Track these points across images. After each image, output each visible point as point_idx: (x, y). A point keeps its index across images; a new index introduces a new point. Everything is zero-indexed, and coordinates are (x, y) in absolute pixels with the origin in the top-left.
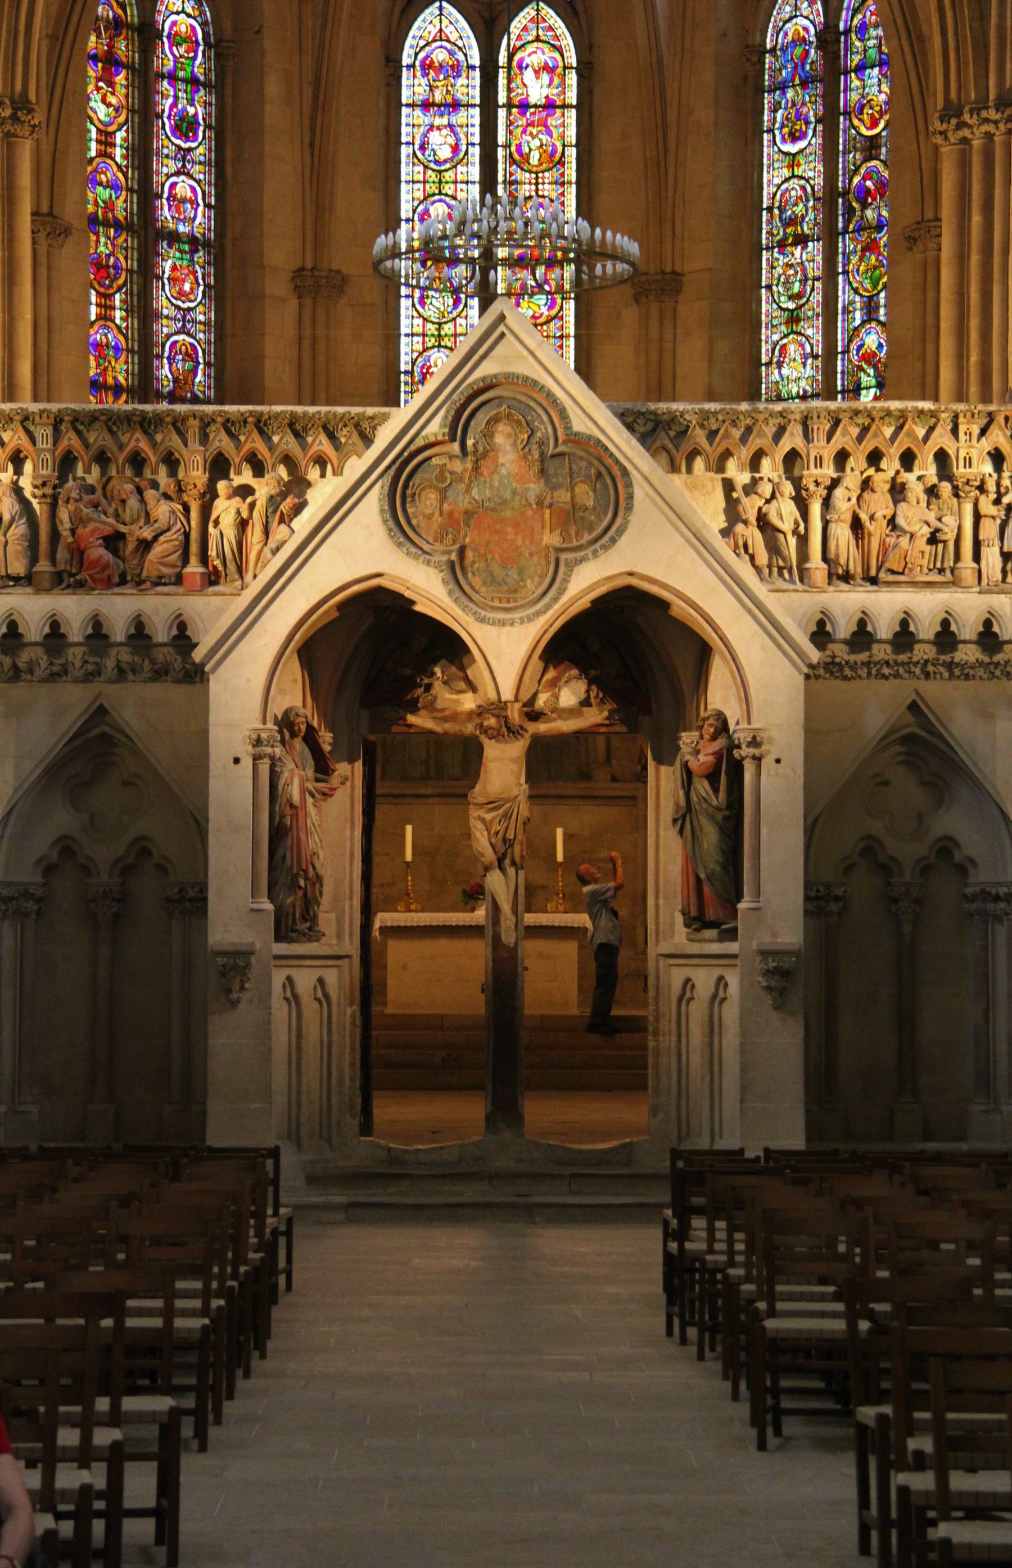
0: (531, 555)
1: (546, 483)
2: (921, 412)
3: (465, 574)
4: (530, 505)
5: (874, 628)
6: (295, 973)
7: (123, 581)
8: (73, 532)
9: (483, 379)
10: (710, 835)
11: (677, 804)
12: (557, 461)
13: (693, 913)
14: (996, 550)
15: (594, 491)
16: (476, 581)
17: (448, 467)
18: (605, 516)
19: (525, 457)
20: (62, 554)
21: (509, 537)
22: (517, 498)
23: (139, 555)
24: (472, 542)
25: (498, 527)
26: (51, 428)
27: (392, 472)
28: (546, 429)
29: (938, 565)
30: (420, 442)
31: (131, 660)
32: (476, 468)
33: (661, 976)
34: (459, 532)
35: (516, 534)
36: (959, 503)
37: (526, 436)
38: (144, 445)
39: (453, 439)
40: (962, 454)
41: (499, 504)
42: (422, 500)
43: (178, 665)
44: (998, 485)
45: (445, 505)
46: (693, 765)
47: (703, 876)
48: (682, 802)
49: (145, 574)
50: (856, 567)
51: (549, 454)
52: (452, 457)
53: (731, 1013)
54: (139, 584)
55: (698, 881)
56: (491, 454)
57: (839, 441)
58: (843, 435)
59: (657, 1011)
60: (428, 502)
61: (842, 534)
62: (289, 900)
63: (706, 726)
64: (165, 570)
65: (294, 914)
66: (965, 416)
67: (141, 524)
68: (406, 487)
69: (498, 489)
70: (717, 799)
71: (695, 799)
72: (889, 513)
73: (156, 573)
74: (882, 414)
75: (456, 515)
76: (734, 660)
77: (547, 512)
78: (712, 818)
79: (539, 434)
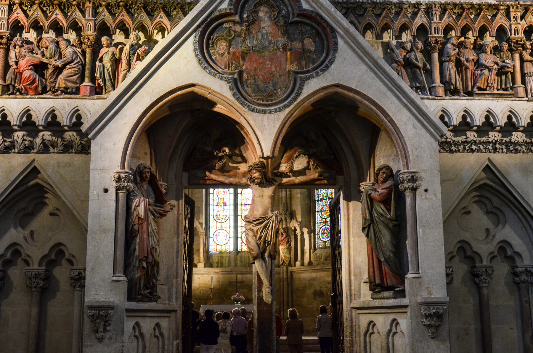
1: (288, 37)
3: (243, 86)
4: (279, 49)
6: (141, 321)
7: (44, 91)
8: (17, 63)
10: (386, 237)
11: (365, 219)
13: (378, 281)
15: (315, 42)
16: (249, 90)
17: (233, 28)
19: (276, 24)
22: (272, 45)
23: (55, 76)
24: (246, 69)
25: (261, 61)
26: (7, 7)
27: (200, 29)
28: (287, 9)
29: (503, 86)
30: (217, 13)
31: (51, 139)
32: (248, 30)
33: (354, 320)
35: (271, 65)
37: (276, 13)
38: (60, 17)
39: (236, 14)
40: (513, 27)
41: (262, 49)
42: (218, 46)
45: (231, 49)
46: (375, 195)
47: (382, 260)
48: (368, 217)
49: (57, 86)
50: (459, 85)
52: (235, 23)
54: (54, 92)
55: (379, 261)
56: (257, 22)
58: (449, 18)
60: (221, 47)
61: (451, 67)
62: (137, 276)
63: (381, 173)
64: (70, 85)
65: (140, 284)
67: (56, 58)
68: (209, 39)
70: (390, 214)
71: (376, 215)
72: (476, 58)
73: (64, 85)
74: (469, 7)
75: (237, 54)
77: (289, 53)
78: (386, 226)
79: (283, 12)
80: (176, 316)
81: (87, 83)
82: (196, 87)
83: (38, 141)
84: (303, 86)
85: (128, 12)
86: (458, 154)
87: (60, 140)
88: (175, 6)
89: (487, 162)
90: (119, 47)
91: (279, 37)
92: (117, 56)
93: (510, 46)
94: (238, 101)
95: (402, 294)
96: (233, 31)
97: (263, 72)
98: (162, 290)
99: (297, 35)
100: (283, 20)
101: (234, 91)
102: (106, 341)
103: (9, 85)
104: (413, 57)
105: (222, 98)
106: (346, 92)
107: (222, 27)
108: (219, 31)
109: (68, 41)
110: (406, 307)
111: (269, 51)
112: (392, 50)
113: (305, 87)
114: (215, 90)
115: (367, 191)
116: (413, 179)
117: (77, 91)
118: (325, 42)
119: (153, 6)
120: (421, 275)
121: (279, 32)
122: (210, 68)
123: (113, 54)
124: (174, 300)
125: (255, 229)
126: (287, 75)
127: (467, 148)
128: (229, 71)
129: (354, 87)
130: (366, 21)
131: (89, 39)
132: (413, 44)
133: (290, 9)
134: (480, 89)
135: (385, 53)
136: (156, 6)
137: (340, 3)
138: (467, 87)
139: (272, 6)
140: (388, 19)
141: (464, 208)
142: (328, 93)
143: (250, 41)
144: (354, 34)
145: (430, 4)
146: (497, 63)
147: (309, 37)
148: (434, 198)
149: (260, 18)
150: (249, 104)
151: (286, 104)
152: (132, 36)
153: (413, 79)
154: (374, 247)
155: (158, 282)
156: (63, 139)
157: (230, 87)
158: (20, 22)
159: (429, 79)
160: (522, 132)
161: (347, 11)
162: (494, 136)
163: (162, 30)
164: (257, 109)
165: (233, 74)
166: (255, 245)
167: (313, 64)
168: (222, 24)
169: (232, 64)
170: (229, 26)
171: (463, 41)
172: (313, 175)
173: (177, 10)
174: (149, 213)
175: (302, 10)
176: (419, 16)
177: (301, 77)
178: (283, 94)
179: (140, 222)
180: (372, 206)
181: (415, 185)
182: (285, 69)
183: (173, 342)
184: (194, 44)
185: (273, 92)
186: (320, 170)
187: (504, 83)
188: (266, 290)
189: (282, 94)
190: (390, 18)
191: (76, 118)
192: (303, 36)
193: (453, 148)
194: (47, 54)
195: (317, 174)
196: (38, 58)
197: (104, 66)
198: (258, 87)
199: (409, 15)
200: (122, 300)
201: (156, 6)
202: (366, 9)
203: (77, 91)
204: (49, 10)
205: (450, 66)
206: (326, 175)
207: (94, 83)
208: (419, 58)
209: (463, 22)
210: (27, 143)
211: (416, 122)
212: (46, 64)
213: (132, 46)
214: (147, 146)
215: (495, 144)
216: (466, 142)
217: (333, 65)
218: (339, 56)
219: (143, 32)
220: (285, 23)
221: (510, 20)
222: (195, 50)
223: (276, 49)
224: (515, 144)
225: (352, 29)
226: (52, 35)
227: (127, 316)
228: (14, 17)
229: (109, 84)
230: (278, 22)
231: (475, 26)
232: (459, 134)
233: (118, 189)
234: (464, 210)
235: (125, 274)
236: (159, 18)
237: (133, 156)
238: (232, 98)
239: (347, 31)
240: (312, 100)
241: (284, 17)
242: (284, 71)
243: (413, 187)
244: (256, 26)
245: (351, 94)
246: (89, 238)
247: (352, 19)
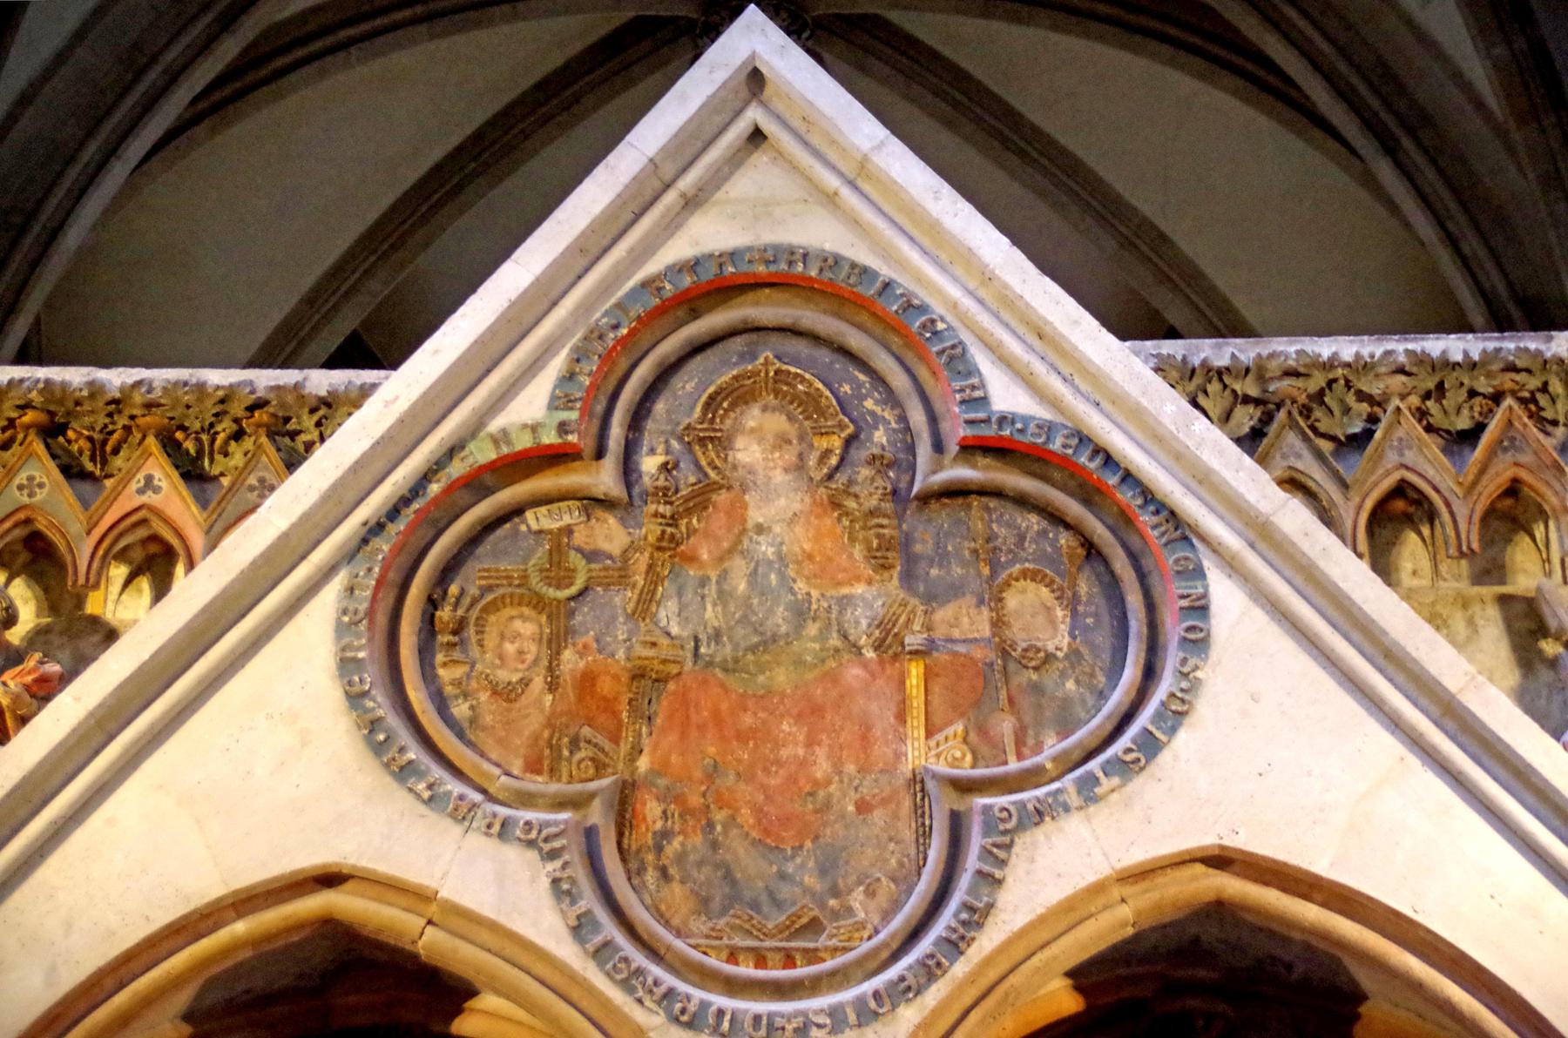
0: (863, 807)
1: (908, 578)
4: (857, 649)
9: (694, 265)
12: (942, 516)
15: (1073, 604)
17: (579, 538)
19: (835, 504)
21: (784, 753)
22: (812, 629)
25: (748, 720)
28: (903, 419)
30: (482, 453)
32: (669, 544)
34: (615, 739)
35: (810, 743)
37: (836, 443)
41: (753, 649)
42: (491, 640)
45: (567, 654)
51: (915, 490)
52: (594, 503)
56: (722, 498)
60: (510, 648)
68: (432, 603)
69: (746, 603)
75: (605, 686)
77: (915, 671)
79: (880, 436)
82: (349, 886)
84: (1003, 863)
88: (236, 421)
91: (858, 579)
94: (601, 964)
96: (579, 550)
97: (764, 788)
99: (963, 563)
100: (879, 482)
101: (583, 905)
107: (516, 533)
108: (496, 554)
114: (468, 901)
118: (1134, 600)
119: (102, 420)
121: (858, 552)
122: (437, 772)
126: (907, 803)
128: (554, 787)
130: (1388, 473)
133: (918, 417)
136: (122, 421)
137: (1220, 373)
139: (810, 405)
140: (1526, 458)
143: (682, 609)
144: (1305, 546)
147: (1033, 576)
149: (741, 472)
150: (670, 980)
151: (902, 979)
157: (556, 882)
164: (721, 1013)
167: (1064, 734)
168: (517, 511)
169: (575, 744)
170: (555, 525)
173: (248, 443)
175: (987, 421)
177: (987, 809)
178: (887, 916)
182: (889, 770)
184: (341, 629)
185: (822, 906)
189: (876, 920)
192: (995, 567)
198: (728, 876)
201: (122, 421)
217: (1182, 735)
222: (347, 665)
223: (837, 650)
225: (1294, 517)
236: (141, 492)
238: (567, 951)
239: (1262, 533)
242: (884, 779)
244: (717, 521)
247: (1293, 462)
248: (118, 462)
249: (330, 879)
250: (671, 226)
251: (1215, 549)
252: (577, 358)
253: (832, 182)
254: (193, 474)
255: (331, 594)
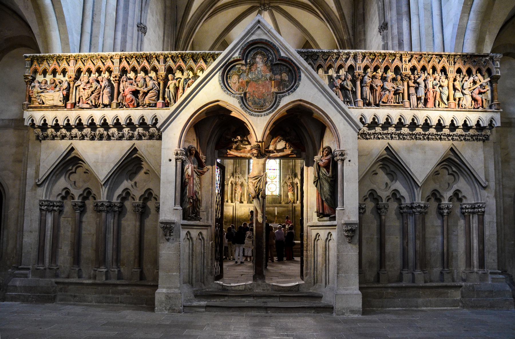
1: (273, 73)
2: (391, 54)
3: (246, 101)
5: (378, 120)
6: (190, 231)
7: (138, 105)
8: (124, 91)
10: (326, 187)
11: (315, 177)
12: (276, 67)
13: (321, 212)
14: (415, 96)
15: (288, 75)
16: (250, 103)
17: (241, 68)
18: (292, 83)
19: (266, 65)
20: (120, 97)
22: (263, 78)
27: (223, 69)
29: (397, 101)
30: (232, 60)
32: (250, 69)
36: (403, 82)
39: (243, 60)
40: (404, 67)
43: (156, 133)
44: (414, 77)
46: (321, 163)
47: (324, 200)
48: (317, 176)
49: (144, 103)
50: (372, 101)
52: (242, 65)
53: (333, 245)
55: (322, 201)
56: (255, 64)
57: (365, 62)
58: (367, 61)
59: (307, 243)
61: (367, 90)
62: (188, 206)
64: (151, 102)
65: (189, 211)
66: (404, 55)
67: (144, 87)
68: (227, 74)
72: (382, 85)
73: (148, 102)
74: (379, 54)
75: (243, 83)
76: (334, 128)
77: (273, 82)
78: (327, 181)
79: (270, 58)
80: (211, 229)
81: (161, 101)
83: (136, 133)
85: (183, 60)
86: (370, 140)
87: (147, 132)
89: (387, 145)
90: (178, 80)
92: (177, 85)
93: (402, 77)
95: (334, 219)
98: (203, 215)
102: (171, 241)
103: (120, 103)
104: (345, 84)
105: (235, 108)
106: (305, 104)
108: (233, 70)
109: (151, 78)
110: (335, 226)
111: (262, 81)
112: (333, 80)
113: (282, 101)
115: (317, 161)
116: (342, 155)
117: (155, 105)
118: (294, 75)
120: (344, 208)
122: (228, 91)
123: (175, 84)
124: (210, 220)
125: (254, 182)
127: (376, 137)
129: (310, 101)
131: (162, 76)
132: (346, 76)
134: (383, 102)
135: (330, 81)
137: (304, 52)
138: (376, 101)
139: (263, 55)
141: (374, 171)
142: (295, 105)
145: (356, 53)
146: (394, 88)
147: (285, 73)
148: (354, 165)
150: (249, 111)
152: (185, 74)
153: (345, 96)
154: (319, 192)
155: (200, 210)
156: (149, 132)
158: (125, 68)
159: (355, 96)
160: (407, 127)
161: (308, 57)
162: (391, 130)
163: (202, 70)
165: (241, 94)
166: (254, 191)
167: (287, 88)
168: (235, 65)
171: (375, 75)
172: (288, 152)
174: (194, 172)
176: (349, 60)
178: (270, 105)
179: (189, 177)
180: (319, 170)
181: (343, 158)
182: (270, 91)
183: (209, 242)
184: (219, 77)
186: (292, 149)
187: (397, 99)
188: (260, 216)
190: (332, 61)
191: (155, 120)
193: (368, 137)
194: (140, 85)
195: (290, 151)
196: (134, 88)
197: (170, 91)
199: (344, 60)
200: (179, 219)
202: (318, 56)
203: (155, 105)
204: (140, 60)
205: (367, 89)
206: (295, 152)
207: (164, 100)
208: (349, 85)
209: (375, 64)
210: (130, 134)
211: (345, 121)
212: (139, 91)
213: (185, 79)
214: (195, 136)
215: (392, 135)
216: (375, 133)
218: (301, 83)
219: (192, 71)
220: (271, 64)
221: (402, 62)
224: (403, 135)
225: (309, 68)
226: (142, 74)
227: (182, 228)
228: (122, 65)
229: (172, 101)
230: (267, 64)
231: (382, 66)
232: (371, 129)
233: (176, 159)
234: (374, 173)
235: (181, 206)
237: (185, 141)
238: (240, 108)
239: (306, 69)
240: (286, 108)
241: (271, 61)
243: (342, 159)
244: (254, 67)
245: (308, 105)
246: (161, 186)
248: (198, 60)
249: (218, 101)
250: (250, 36)
251: (302, 70)
252: (241, 50)
253: (266, 32)
254: (205, 61)
255: (218, 73)
